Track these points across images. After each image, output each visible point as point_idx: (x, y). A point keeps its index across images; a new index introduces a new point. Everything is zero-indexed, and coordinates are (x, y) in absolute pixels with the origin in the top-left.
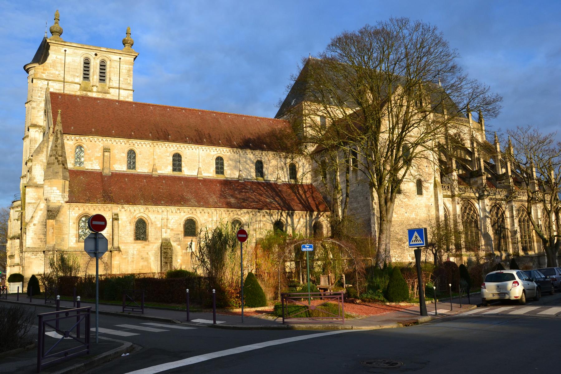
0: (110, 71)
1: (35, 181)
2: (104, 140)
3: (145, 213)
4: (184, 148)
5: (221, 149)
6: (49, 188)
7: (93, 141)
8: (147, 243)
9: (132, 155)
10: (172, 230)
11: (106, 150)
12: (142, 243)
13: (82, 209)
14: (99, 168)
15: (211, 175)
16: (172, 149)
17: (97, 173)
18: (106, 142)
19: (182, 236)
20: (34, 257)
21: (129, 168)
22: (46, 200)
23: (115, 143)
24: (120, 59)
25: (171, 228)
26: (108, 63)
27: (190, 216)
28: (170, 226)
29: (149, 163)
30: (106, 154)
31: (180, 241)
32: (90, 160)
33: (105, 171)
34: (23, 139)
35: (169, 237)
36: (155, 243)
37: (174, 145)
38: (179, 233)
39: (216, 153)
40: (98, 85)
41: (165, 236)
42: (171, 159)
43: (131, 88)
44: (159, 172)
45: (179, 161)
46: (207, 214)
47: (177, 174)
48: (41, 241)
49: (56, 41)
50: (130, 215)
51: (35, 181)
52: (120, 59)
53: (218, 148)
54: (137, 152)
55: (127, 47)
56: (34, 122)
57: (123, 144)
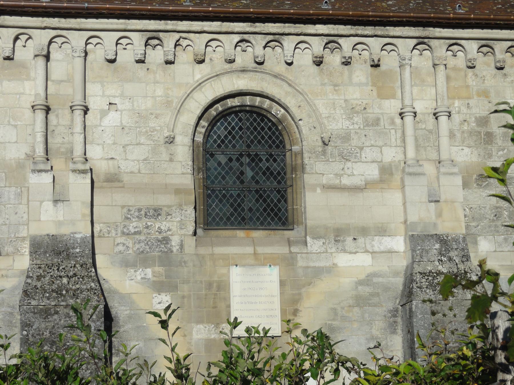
19: (180, 223)
31: (167, 259)
38: (164, 200)
41: (52, 220)
46: (360, 73)
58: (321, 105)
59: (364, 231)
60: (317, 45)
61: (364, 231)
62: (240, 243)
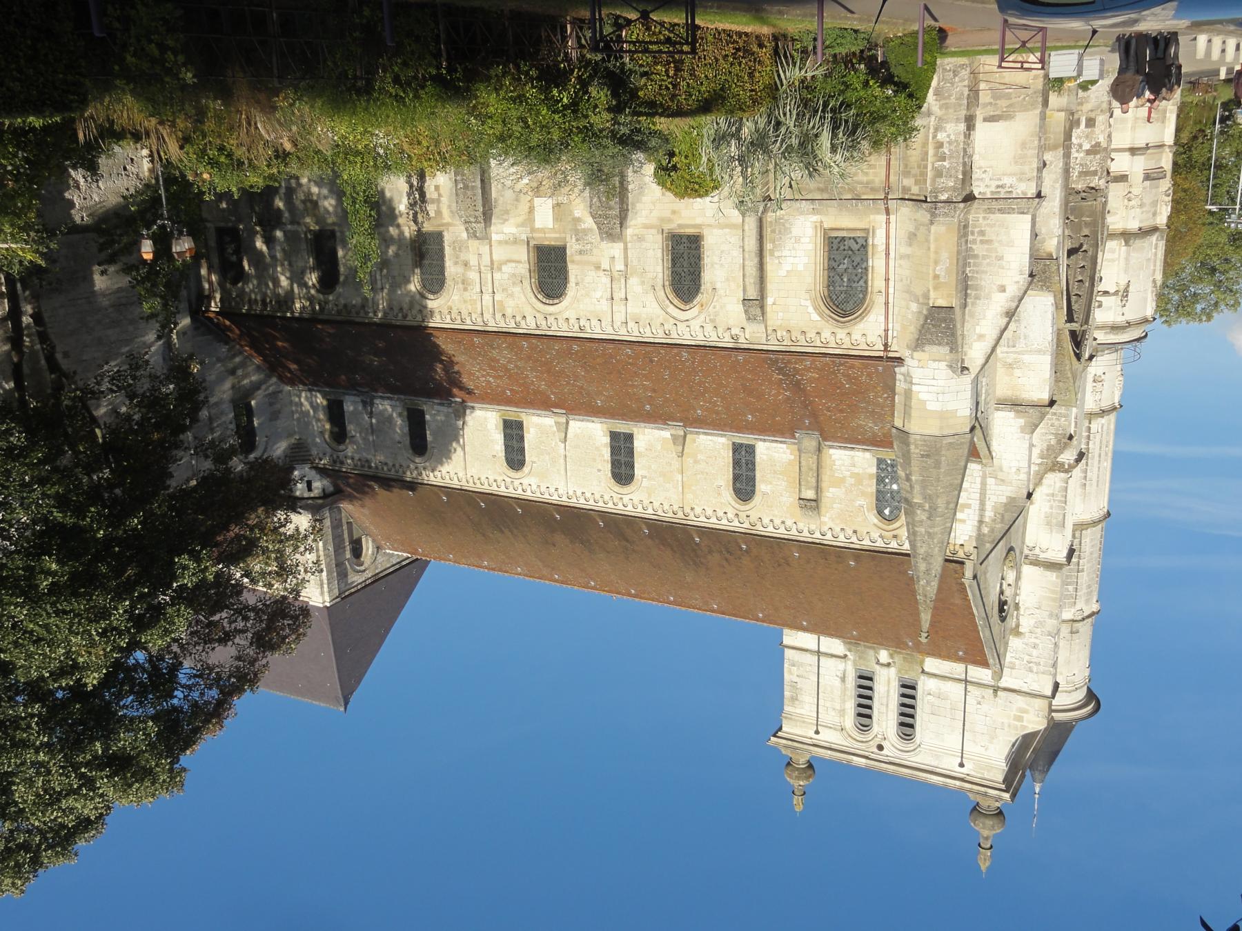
0: (843, 701)
1: (1022, 421)
2: (818, 535)
3: (672, 321)
4: (607, 498)
5: (511, 490)
6: (950, 407)
7: (849, 532)
8: (667, 227)
9: (744, 483)
10: (598, 268)
11: (812, 505)
12: (680, 226)
13: (856, 336)
14: (832, 451)
15: (535, 419)
16: (636, 498)
17: (835, 439)
18: (813, 527)
20: (1007, 181)
21: (751, 450)
22: (964, 369)
23: (789, 523)
24: (817, 732)
25: (601, 273)
26: (849, 720)
27: (551, 309)
28: (606, 280)
29: (696, 462)
30: (810, 494)
31: (577, 232)
32: (858, 478)
33: (814, 443)
34: (1109, 514)
35: (605, 245)
36: (646, 227)
37: (630, 508)
38: (577, 258)
39: (525, 481)
40: (877, 667)
41: (616, 249)
42: (638, 471)
43: (788, 653)
44: (666, 434)
45: (619, 461)
46: (509, 312)
47: (622, 427)
48: (982, 233)
49: (985, 795)
50: (716, 314)
51: (1022, 421)
52: (817, 732)
53: (519, 493)
54: (728, 495)
55: (802, 760)
56: (1052, 576)
57: (766, 521)
58: (523, 299)
59: (506, 242)
60: (523, 324)
61: (506, 242)
62: (551, 239)
